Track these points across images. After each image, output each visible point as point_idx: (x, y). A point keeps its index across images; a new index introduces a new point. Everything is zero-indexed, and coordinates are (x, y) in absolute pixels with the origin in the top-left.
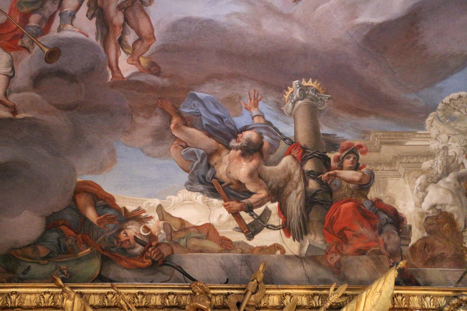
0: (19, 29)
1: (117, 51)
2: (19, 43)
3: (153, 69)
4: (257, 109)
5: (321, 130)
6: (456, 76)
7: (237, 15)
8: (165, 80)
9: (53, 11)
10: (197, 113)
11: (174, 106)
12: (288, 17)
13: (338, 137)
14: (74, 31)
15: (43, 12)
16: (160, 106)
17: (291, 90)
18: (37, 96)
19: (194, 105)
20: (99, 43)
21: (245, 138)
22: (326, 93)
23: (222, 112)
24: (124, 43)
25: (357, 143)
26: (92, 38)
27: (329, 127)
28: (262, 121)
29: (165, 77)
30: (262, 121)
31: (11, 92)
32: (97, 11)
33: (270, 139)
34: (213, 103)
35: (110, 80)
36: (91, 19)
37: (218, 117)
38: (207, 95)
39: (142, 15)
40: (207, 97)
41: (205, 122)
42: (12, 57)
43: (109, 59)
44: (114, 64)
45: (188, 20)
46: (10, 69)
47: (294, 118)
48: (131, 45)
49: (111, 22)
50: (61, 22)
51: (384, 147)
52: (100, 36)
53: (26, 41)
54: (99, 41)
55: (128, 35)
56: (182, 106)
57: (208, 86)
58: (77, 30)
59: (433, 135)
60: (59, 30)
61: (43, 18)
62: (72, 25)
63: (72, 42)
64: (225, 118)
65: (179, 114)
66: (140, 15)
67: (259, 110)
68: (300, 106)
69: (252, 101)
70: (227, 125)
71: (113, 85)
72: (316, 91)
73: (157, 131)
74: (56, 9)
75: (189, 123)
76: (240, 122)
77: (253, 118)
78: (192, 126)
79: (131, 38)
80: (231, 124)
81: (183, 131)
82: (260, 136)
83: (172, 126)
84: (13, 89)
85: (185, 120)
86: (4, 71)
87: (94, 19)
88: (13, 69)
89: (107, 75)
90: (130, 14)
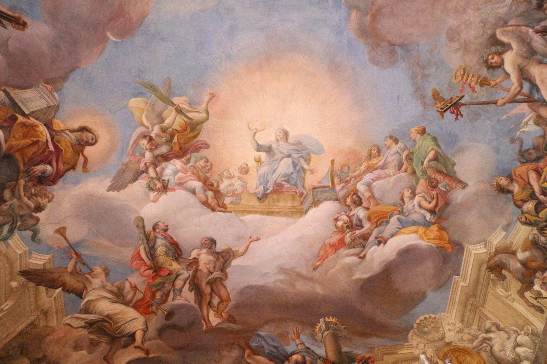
0: (150, 302)
1: (208, 310)
2: (150, 310)
3: (230, 319)
4: (299, 340)
5: (342, 349)
6: (420, 305)
7: (280, 281)
8: (239, 326)
9: (170, 288)
10: (261, 345)
11: (246, 342)
12: (311, 279)
13: (355, 353)
14: (181, 300)
15: (164, 290)
16: (237, 343)
17: (319, 325)
18: (161, 342)
19: (259, 341)
20: (196, 306)
21: (294, 359)
22: (342, 325)
23: (276, 344)
24: (212, 304)
25: (367, 356)
26: (193, 303)
27: (347, 347)
28: (303, 347)
29: (239, 324)
30: (303, 347)
31: (145, 341)
32: (194, 287)
33: (310, 359)
34: (271, 339)
35: (204, 329)
36: (191, 291)
37: (275, 347)
38: (267, 333)
39: (222, 287)
40: (267, 334)
41: (267, 351)
42: (146, 319)
43: (203, 315)
44: (206, 318)
45: (250, 287)
46: (145, 326)
47: (324, 343)
48: (216, 305)
49: (204, 292)
50: (174, 295)
52: (197, 301)
53: (154, 308)
54: (197, 304)
55: (214, 299)
56: (251, 342)
57: (267, 327)
58: (183, 299)
59: (415, 345)
60: (173, 300)
61: (164, 293)
62: (180, 296)
63: (181, 307)
64: (279, 347)
65: (250, 347)
66: (221, 287)
67: (301, 340)
68: (327, 335)
69: (296, 334)
70: (281, 352)
71: (207, 332)
72: (336, 324)
73: (236, 359)
74: (171, 287)
75: (256, 352)
76: (290, 349)
77: (297, 346)
78: (259, 355)
79: (216, 301)
80: (283, 351)
81: (253, 359)
82: (304, 357)
83: (246, 356)
84: (147, 339)
85: (254, 350)
86: (142, 328)
87: (193, 292)
88: (147, 326)
89: (203, 325)
90: (215, 287)
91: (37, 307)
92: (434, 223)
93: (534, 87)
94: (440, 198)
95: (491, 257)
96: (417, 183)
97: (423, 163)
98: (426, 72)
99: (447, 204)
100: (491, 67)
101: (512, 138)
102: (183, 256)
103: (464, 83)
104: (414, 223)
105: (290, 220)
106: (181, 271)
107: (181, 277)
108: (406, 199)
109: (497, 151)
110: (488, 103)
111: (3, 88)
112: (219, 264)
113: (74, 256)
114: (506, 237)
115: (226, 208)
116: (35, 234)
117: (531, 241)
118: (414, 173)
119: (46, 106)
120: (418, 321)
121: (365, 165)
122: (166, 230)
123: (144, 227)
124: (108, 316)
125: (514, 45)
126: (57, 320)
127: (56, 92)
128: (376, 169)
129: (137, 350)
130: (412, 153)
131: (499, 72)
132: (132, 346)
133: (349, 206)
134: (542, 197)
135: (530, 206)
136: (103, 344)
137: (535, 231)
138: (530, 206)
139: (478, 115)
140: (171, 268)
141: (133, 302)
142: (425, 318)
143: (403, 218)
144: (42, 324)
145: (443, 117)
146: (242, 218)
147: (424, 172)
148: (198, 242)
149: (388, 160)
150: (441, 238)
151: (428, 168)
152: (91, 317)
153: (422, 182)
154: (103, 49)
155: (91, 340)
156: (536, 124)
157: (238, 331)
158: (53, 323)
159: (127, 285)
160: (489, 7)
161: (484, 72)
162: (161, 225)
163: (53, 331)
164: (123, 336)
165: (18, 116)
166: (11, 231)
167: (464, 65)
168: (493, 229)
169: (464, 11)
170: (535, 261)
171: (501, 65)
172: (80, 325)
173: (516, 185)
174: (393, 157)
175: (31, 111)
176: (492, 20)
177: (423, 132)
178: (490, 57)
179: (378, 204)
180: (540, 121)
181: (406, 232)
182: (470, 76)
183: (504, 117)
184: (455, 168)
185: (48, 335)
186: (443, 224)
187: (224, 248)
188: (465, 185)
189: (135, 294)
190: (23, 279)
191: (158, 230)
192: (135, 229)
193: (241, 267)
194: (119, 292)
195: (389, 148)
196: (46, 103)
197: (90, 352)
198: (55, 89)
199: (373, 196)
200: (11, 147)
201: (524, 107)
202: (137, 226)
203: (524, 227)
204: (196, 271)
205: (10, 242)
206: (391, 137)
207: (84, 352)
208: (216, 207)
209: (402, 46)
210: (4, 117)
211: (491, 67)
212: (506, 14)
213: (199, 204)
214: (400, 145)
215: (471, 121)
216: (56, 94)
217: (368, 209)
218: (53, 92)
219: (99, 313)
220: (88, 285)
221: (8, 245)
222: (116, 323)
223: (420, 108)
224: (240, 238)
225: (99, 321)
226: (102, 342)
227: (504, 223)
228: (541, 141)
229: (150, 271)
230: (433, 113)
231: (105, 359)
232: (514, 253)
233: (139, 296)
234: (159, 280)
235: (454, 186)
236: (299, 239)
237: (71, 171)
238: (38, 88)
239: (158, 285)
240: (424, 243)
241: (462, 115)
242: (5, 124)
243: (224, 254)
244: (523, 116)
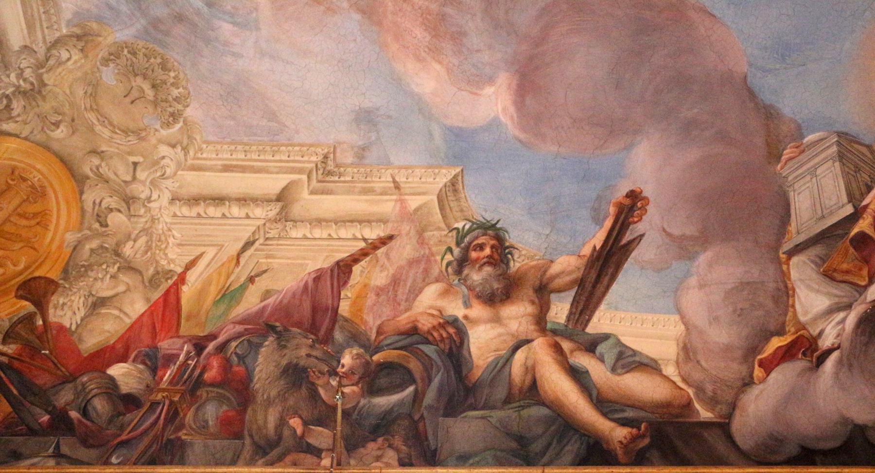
111: (783, 257)
119: (837, 164)
127: (804, 138)
165: (855, 231)
175: (845, 199)
196: (830, 163)
198: (794, 140)
210: (856, 262)
216: (810, 138)
218: (802, 144)
238: (790, 178)
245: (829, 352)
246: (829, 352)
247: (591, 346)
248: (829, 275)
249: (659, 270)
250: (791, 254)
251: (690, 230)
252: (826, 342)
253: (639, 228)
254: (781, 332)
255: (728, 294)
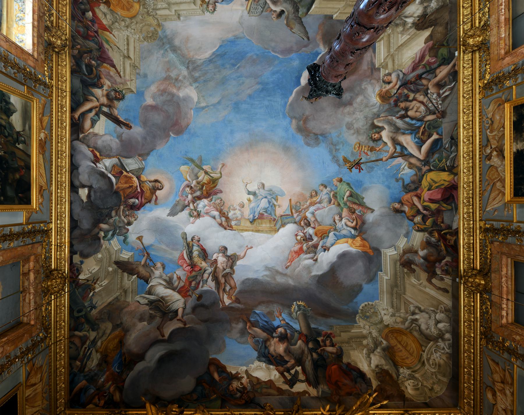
1: (223, 294)
12: (285, 275)
17: (294, 307)
18: (194, 316)
20: (216, 291)
22: (309, 307)
25: (329, 332)
26: (214, 289)
45: (248, 279)
51: (342, 334)
53: (190, 293)
57: (260, 307)
60: (202, 287)
61: (197, 283)
63: (206, 292)
68: (299, 314)
72: (304, 307)
79: (228, 288)
82: (285, 330)
90: (227, 279)
91: (121, 287)
92: (357, 236)
93: (403, 147)
94: (358, 219)
95: (401, 257)
96: (342, 211)
97: (343, 199)
98: (338, 148)
99: (364, 223)
100: (374, 140)
101: (396, 179)
102: (209, 258)
103: (361, 151)
104: (345, 236)
105: (269, 235)
106: (207, 268)
107: (207, 272)
108: (337, 221)
109: (389, 187)
110: (377, 160)
112: (229, 264)
113: (146, 255)
114: (408, 241)
115: (232, 228)
116: (126, 238)
117: (426, 242)
118: (339, 205)
120: (361, 308)
121: (309, 201)
122: (199, 241)
123: (186, 239)
124: (162, 298)
125: (386, 127)
126: (132, 298)
128: (316, 204)
129: (178, 322)
130: (336, 193)
131: (380, 142)
132: (175, 319)
133: (303, 227)
134: (425, 212)
135: (418, 219)
136: (158, 318)
137: (426, 235)
138: (419, 219)
139: (372, 168)
140: (201, 266)
141: (178, 289)
142: (366, 305)
143: (337, 233)
144: (123, 299)
145: (351, 171)
146: (241, 234)
147: (345, 204)
148: (217, 249)
149: (322, 198)
150: (364, 246)
151: (347, 201)
152: (152, 297)
153: (345, 210)
154: (168, 141)
155: (151, 314)
156: (409, 168)
157: (242, 309)
158: (129, 299)
159: (175, 276)
160: (367, 109)
161: (371, 144)
162: (196, 238)
163: (129, 305)
164: (171, 312)
166: (113, 235)
167: (358, 141)
168: (398, 237)
169: (354, 113)
170: (432, 256)
171: (380, 138)
172: (145, 303)
173: (406, 207)
174: (325, 196)
176: (370, 115)
177: (341, 180)
178: (373, 135)
179: (320, 225)
180: (412, 166)
181: (341, 242)
182: (364, 147)
183: (389, 167)
184: (364, 200)
185: (125, 308)
186: (364, 236)
187: (232, 253)
188: (373, 211)
189: (179, 283)
190: (115, 267)
191: (194, 241)
192: (182, 239)
193: (244, 266)
194: (170, 281)
195: (322, 191)
197: (149, 324)
199: (316, 220)
200: (118, 188)
201: (400, 160)
202: (183, 238)
203: (418, 233)
204: (216, 268)
205: (112, 242)
206: (322, 185)
207: (145, 323)
208: (227, 227)
209: (322, 135)
211: (374, 140)
212: (378, 111)
213: (217, 225)
214: (328, 189)
215: (369, 172)
216: (143, 162)
217: (314, 228)
219: (157, 295)
220: (152, 275)
221: (110, 244)
222: (167, 303)
223: (337, 167)
224: (241, 247)
225: (157, 301)
226: (157, 316)
227: (404, 232)
228: (415, 178)
229: (189, 268)
230: (345, 170)
231: (158, 328)
232: (416, 252)
233: (182, 284)
234: (194, 273)
235: (366, 211)
236: (276, 248)
237: (148, 204)
239: (193, 277)
240: (353, 250)
241: (362, 169)
242: (117, 175)
243: (232, 257)
244: (400, 165)
245: (96, 165)
246: (96, 165)
247: (97, 114)
248: (114, 166)
249: (115, 131)
250: (118, 158)
251: (123, 138)
252: (98, 164)
253: (124, 128)
254: (100, 155)
255: (109, 145)
